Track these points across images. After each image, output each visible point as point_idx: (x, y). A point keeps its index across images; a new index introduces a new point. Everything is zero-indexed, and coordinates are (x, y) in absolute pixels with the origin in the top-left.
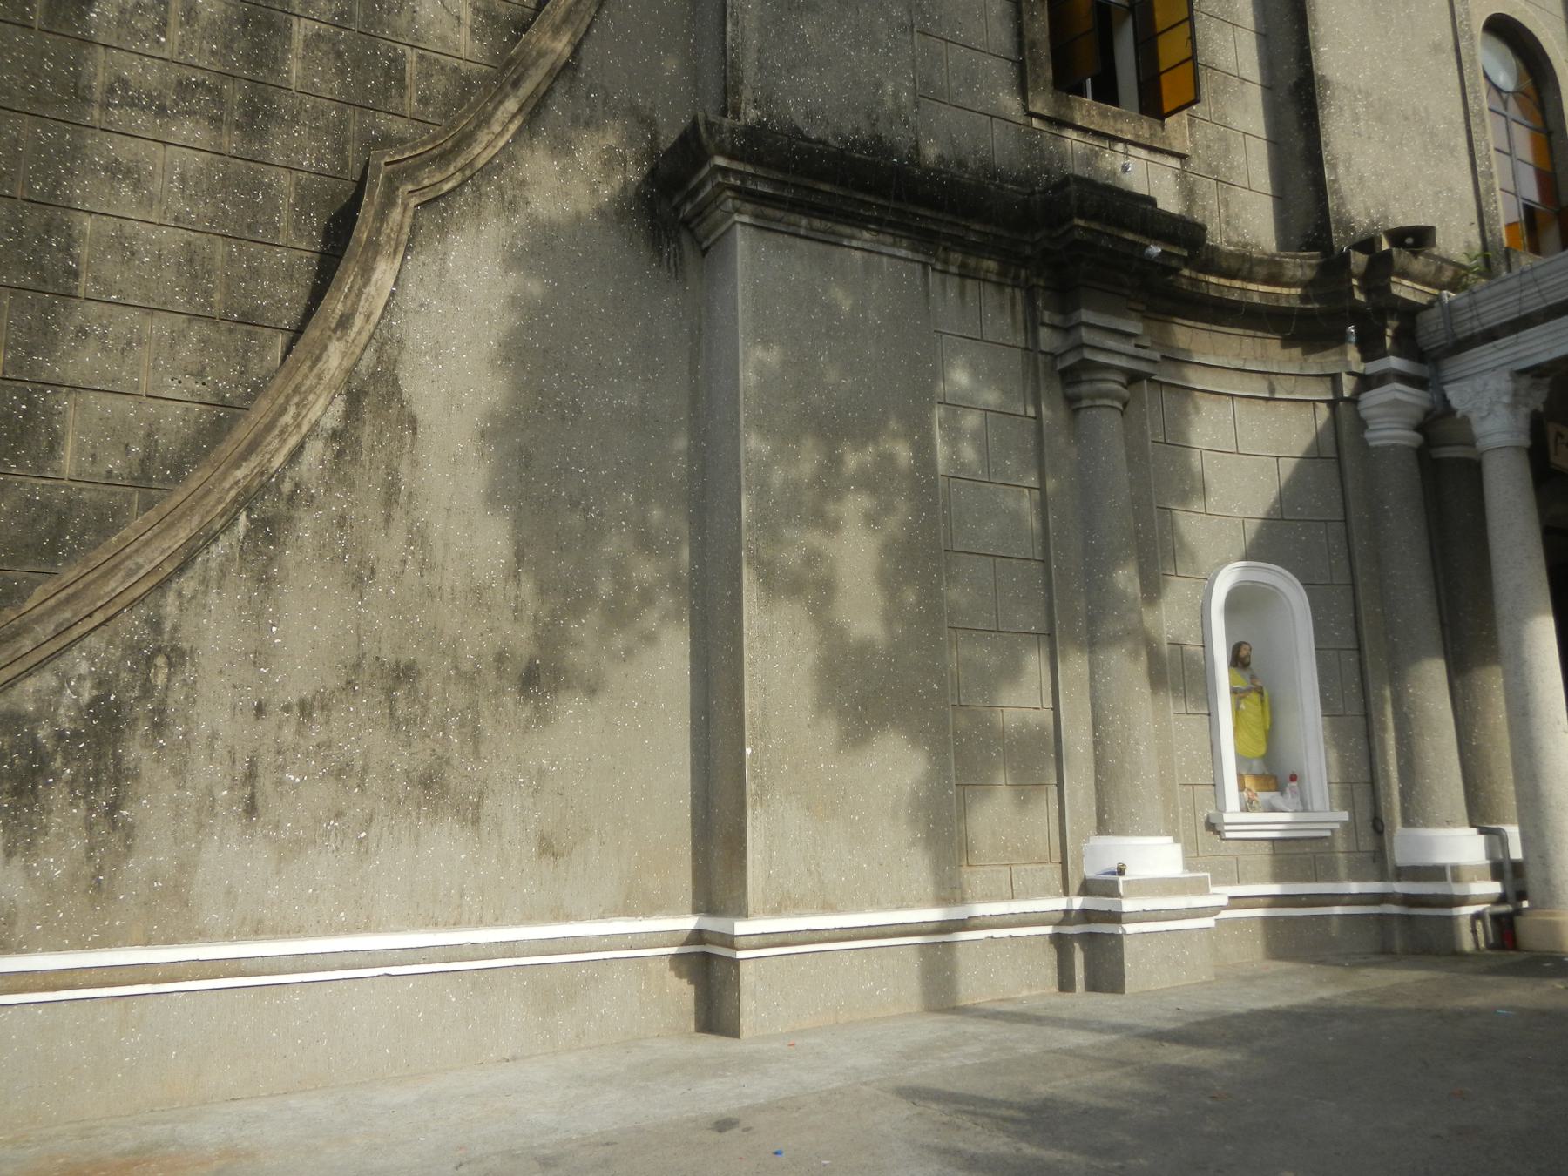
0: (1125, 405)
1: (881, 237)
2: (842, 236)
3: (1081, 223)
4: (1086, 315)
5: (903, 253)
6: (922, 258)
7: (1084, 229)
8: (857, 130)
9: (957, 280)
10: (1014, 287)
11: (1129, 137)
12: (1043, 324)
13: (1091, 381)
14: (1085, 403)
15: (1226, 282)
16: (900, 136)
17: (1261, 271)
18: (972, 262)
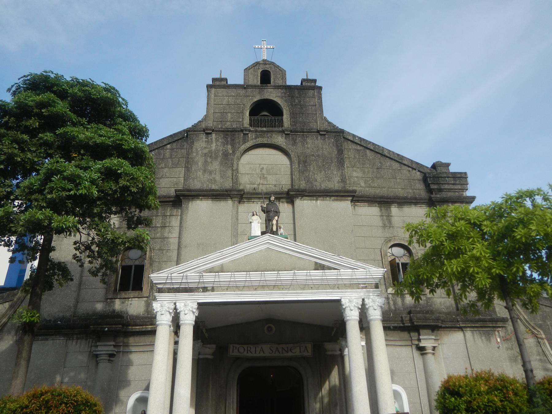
0: (109, 360)
1: (57, 337)
2: (49, 338)
3: (92, 327)
4: (98, 344)
5: (62, 338)
6: (66, 338)
7: (93, 328)
8: (58, 316)
9: (76, 340)
10: (90, 339)
11: (132, 297)
12: (93, 346)
13: (99, 357)
14: (99, 362)
15: (141, 327)
16: (68, 314)
17: (148, 323)
18: (79, 336)
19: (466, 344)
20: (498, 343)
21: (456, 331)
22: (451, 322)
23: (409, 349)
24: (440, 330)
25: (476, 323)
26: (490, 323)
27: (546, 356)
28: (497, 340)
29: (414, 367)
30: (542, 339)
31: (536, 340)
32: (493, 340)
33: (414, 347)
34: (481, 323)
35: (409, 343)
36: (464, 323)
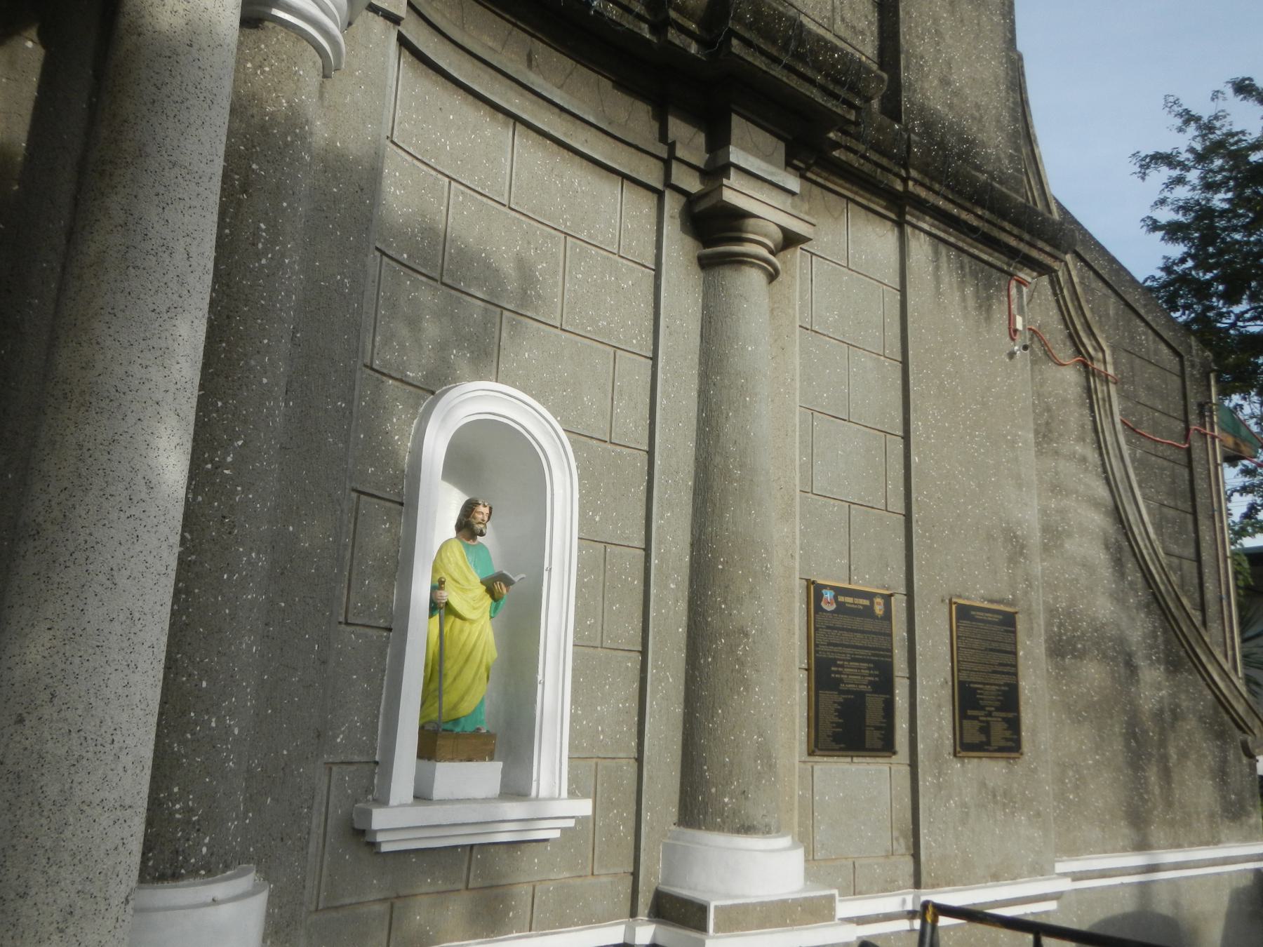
19: (903, 291)
20: (1013, 332)
21: (871, 215)
22: (876, 147)
23: (645, 206)
24: (809, 175)
25: (968, 205)
26: (1016, 231)
27: (1100, 448)
28: (1011, 320)
29: (649, 324)
30: (1105, 379)
31: (1082, 380)
32: (1000, 317)
33: (673, 204)
34: (987, 214)
35: (650, 173)
36: (927, 181)
